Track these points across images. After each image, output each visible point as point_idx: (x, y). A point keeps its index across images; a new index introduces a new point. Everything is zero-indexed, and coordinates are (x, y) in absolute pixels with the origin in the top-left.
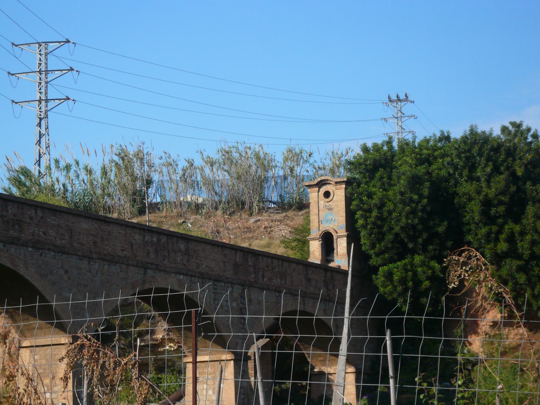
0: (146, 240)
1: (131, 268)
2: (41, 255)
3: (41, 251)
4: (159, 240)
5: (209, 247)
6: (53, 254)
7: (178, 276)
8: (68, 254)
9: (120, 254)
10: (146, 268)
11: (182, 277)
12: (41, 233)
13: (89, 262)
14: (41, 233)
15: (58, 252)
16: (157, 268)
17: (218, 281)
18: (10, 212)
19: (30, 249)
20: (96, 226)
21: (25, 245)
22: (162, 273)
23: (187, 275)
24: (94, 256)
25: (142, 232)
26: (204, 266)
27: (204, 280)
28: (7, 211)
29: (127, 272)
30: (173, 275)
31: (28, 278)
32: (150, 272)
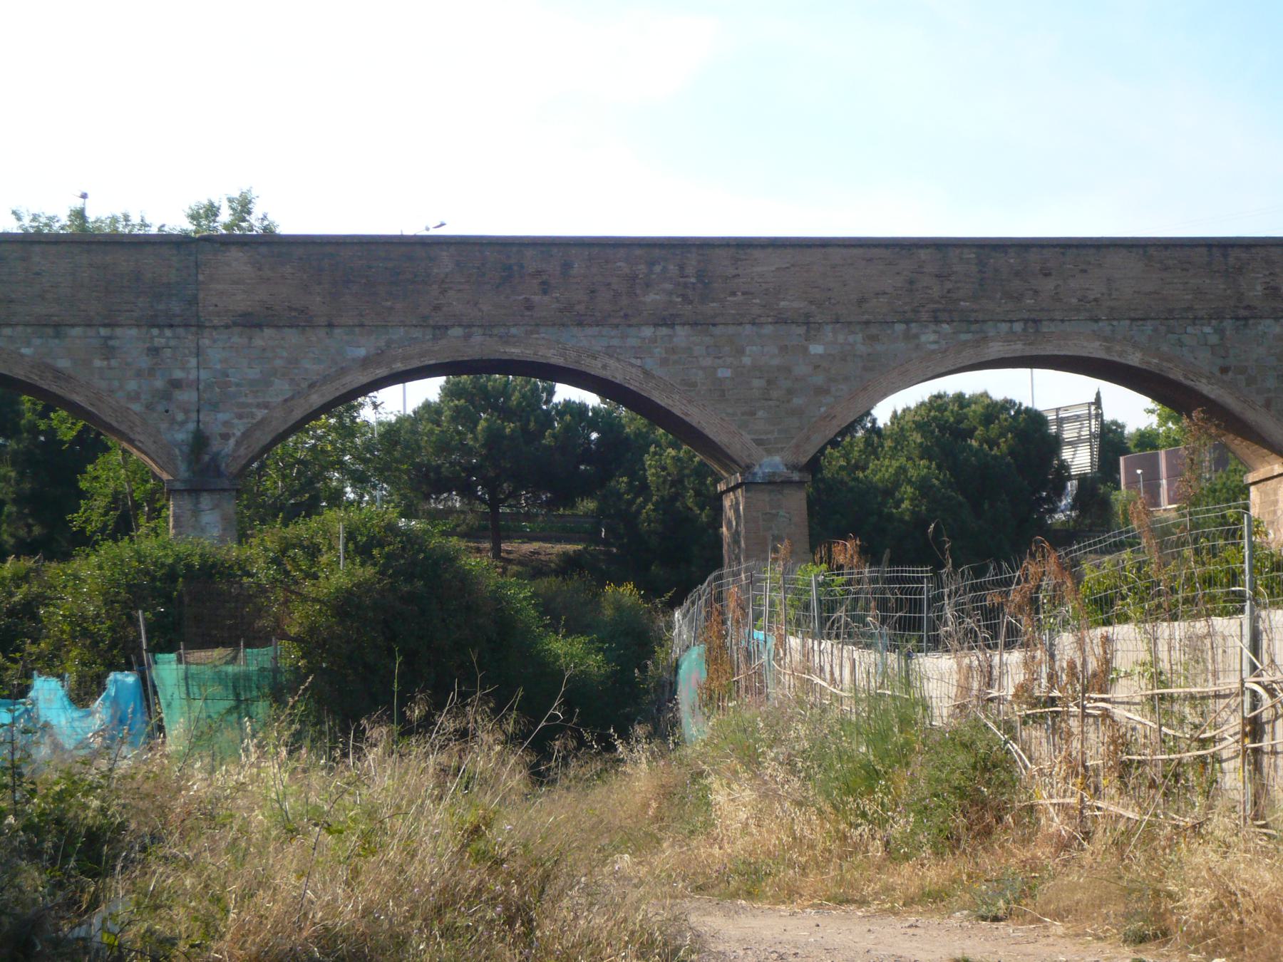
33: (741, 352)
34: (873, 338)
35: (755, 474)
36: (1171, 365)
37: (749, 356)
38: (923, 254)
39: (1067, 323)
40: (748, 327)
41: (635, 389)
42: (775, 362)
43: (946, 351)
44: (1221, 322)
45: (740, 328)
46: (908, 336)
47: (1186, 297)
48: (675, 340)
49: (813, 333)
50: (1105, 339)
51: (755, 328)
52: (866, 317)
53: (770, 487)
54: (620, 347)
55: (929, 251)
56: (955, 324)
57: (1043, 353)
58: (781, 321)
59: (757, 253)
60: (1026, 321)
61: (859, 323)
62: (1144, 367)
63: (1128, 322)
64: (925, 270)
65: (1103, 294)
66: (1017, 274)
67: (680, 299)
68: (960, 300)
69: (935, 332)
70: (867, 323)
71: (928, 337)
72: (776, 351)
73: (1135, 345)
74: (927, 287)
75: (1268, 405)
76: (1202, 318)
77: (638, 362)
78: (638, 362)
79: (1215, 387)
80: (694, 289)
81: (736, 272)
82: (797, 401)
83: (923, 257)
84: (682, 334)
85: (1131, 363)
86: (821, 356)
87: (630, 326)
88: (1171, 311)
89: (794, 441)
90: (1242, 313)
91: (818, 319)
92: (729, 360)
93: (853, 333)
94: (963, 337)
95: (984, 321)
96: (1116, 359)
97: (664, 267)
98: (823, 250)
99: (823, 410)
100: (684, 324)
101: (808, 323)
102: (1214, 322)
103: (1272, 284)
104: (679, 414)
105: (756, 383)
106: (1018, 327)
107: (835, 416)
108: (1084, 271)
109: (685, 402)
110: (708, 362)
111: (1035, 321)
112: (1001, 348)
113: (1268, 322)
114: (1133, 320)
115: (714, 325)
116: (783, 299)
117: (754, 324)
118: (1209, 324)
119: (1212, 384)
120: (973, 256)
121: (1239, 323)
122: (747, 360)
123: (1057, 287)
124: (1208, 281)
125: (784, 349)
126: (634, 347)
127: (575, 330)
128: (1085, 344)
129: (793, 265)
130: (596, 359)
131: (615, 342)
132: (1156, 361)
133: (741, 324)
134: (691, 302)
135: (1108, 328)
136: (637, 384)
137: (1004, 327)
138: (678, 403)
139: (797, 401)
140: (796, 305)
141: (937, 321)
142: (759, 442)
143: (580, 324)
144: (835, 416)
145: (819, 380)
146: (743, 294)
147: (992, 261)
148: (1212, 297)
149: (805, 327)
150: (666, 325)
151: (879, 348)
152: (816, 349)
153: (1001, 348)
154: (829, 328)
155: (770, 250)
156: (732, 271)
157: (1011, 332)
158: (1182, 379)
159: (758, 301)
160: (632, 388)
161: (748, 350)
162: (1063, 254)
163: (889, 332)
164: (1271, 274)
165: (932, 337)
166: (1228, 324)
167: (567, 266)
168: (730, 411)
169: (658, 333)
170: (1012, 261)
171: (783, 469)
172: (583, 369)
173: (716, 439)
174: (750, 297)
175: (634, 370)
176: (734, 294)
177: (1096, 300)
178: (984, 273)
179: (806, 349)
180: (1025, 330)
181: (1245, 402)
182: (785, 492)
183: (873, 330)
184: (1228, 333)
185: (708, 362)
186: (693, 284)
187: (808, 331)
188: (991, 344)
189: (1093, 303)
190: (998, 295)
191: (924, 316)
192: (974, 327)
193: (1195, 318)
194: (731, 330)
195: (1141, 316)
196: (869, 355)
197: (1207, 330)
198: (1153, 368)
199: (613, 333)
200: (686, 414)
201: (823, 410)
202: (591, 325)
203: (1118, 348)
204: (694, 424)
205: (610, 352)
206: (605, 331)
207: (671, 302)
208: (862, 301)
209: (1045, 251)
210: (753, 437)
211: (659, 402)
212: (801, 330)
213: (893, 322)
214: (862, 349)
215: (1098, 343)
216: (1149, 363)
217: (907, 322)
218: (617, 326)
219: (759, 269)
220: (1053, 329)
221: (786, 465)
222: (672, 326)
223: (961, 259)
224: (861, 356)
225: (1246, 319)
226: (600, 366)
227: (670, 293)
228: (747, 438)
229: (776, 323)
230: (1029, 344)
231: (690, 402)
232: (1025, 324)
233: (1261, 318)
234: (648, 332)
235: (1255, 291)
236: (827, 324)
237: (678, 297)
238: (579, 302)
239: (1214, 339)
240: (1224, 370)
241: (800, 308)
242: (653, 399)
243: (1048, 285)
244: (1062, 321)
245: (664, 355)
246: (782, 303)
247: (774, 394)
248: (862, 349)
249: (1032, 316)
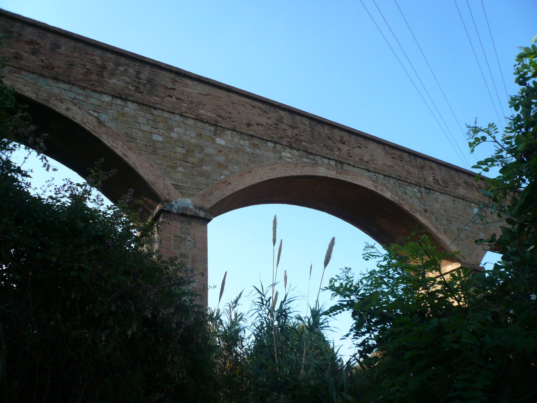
33: (170, 129)
34: (256, 146)
35: (172, 206)
36: (404, 203)
37: (177, 133)
39: (356, 168)
40: (178, 117)
41: (89, 129)
42: (193, 141)
43: (296, 164)
44: (421, 188)
45: (172, 116)
46: (274, 150)
47: (404, 173)
48: (126, 109)
49: (219, 132)
50: (374, 181)
51: (182, 119)
52: (251, 133)
53: (182, 218)
54: (83, 101)
55: (285, 113)
56: (300, 152)
57: (346, 180)
58: (199, 119)
59: (188, 82)
61: (247, 135)
62: (392, 200)
63: (382, 176)
64: (283, 121)
65: (369, 160)
66: (330, 139)
67: (133, 88)
68: (303, 141)
69: (289, 152)
70: (252, 136)
71: (286, 154)
72: (195, 136)
73: (387, 188)
74: (285, 129)
75: (445, 232)
76: (413, 184)
77: (96, 114)
78: (96, 114)
79: (423, 218)
80: (144, 86)
81: (173, 87)
82: (206, 168)
83: (282, 115)
84: (131, 108)
85: (387, 197)
86: (223, 146)
87: (94, 91)
88: (400, 176)
89: (202, 192)
91: (223, 125)
92: (162, 132)
93: (243, 139)
94: (305, 160)
95: (316, 155)
96: (380, 193)
97: (126, 69)
98: (228, 93)
99: (222, 177)
100: (134, 102)
101: (216, 126)
102: (418, 187)
103: (435, 178)
104: (120, 154)
105: (179, 150)
107: (230, 183)
109: (125, 147)
110: (147, 128)
111: (340, 162)
112: (325, 171)
113: (438, 193)
114: (385, 175)
115: (155, 109)
116: (202, 109)
117: (181, 116)
118: (416, 188)
119: (422, 216)
120: (308, 123)
121: (427, 191)
122: (174, 135)
123: (349, 150)
124: (411, 169)
125: (200, 135)
126: (94, 105)
127: (50, 82)
128: (365, 181)
129: (209, 95)
130: (62, 103)
131: (81, 98)
132: (397, 198)
133: (173, 113)
134: (141, 92)
135: (375, 177)
136: (91, 127)
137: (326, 161)
138: (120, 147)
139: (206, 168)
140: (209, 114)
142: (177, 187)
143: (56, 79)
144: (230, 183)
145: (221, 159)
146: (177, 98)
147: (317, 128)
148: (414, 176)
149: (214, 128)
150: (121, 98)
151: (258, 152)
152: (220, 141)
153: (325, 171)
154: (229, 132)
155: (196, 83)
156: (170, 85)
157: (329, 164)
158: (409, 210)
159: (185, 105)
160: (86, 128)
161: (176, 129)
162: (350, 136)
163: (264, 145)
164: (434, 174)
165: (289, 155)
167: (55, 46)
168: (158, 161)
169: (113, 102)
170: (327, 131)
171: (191, 207)
172: (50, 105)
173: (146, 177)
174: (180, 101)
175: (91, 118)
176: (171, 97)
177: (367, 161)
178: (314, 132)
179: (214, 140)
180: (336, 165)
181: (436, 228)
182: (193, 224)
183: (256, 141)
184: (424, 194)
185: (147, 128)
186: (144, 83)
187: (216, 129)
188: (320, 168)
189: (366, 163)
190: (322, 145)
192: (310, 156)
194: (166, 115)
195: (388, 175)
196: (252, 154)
198: (396, 202)
199: (81, 92)
200: (125, 156)
201: (222, 177)
202: (64, 82)
203: (380, 187)
204: (131, 163)
205: (75, 102)
206: (75, 89)
207: (127, 88)
208: (249, 125)
209: (342, 132)
210: (173, 182)
211: (106, 142)
212: (212, 129)
213: (267, 141)
214: (249, 150)
215: (371, 182)
216: (394, 199)
217: (275, 143)
218: (84, 88)
219: (188, 90)
220: (349, 169)
221: (195, 206)
222: (126, 100)
223: (302, 122)
224: (248, 153)
225: (429, 189)
226: (64, 107)
227: (128, 83)
228: (168, 182)
229: (197, 119)
230: (339, 173)
231: (129, 149)
232: (336, 163)
233: (435, 191)
234: (107, 99)
236: (228, 129)
237: (132, 86)
238: (59, 67)
239: (419, 195)
241: (211, 117)
242: (102, 139)
243: (345, 148)
244: (354, 166)
245: (116, 115)
246: (201, 111)
247: (191, 159)
248: (249, 150)
249: (339, 159)
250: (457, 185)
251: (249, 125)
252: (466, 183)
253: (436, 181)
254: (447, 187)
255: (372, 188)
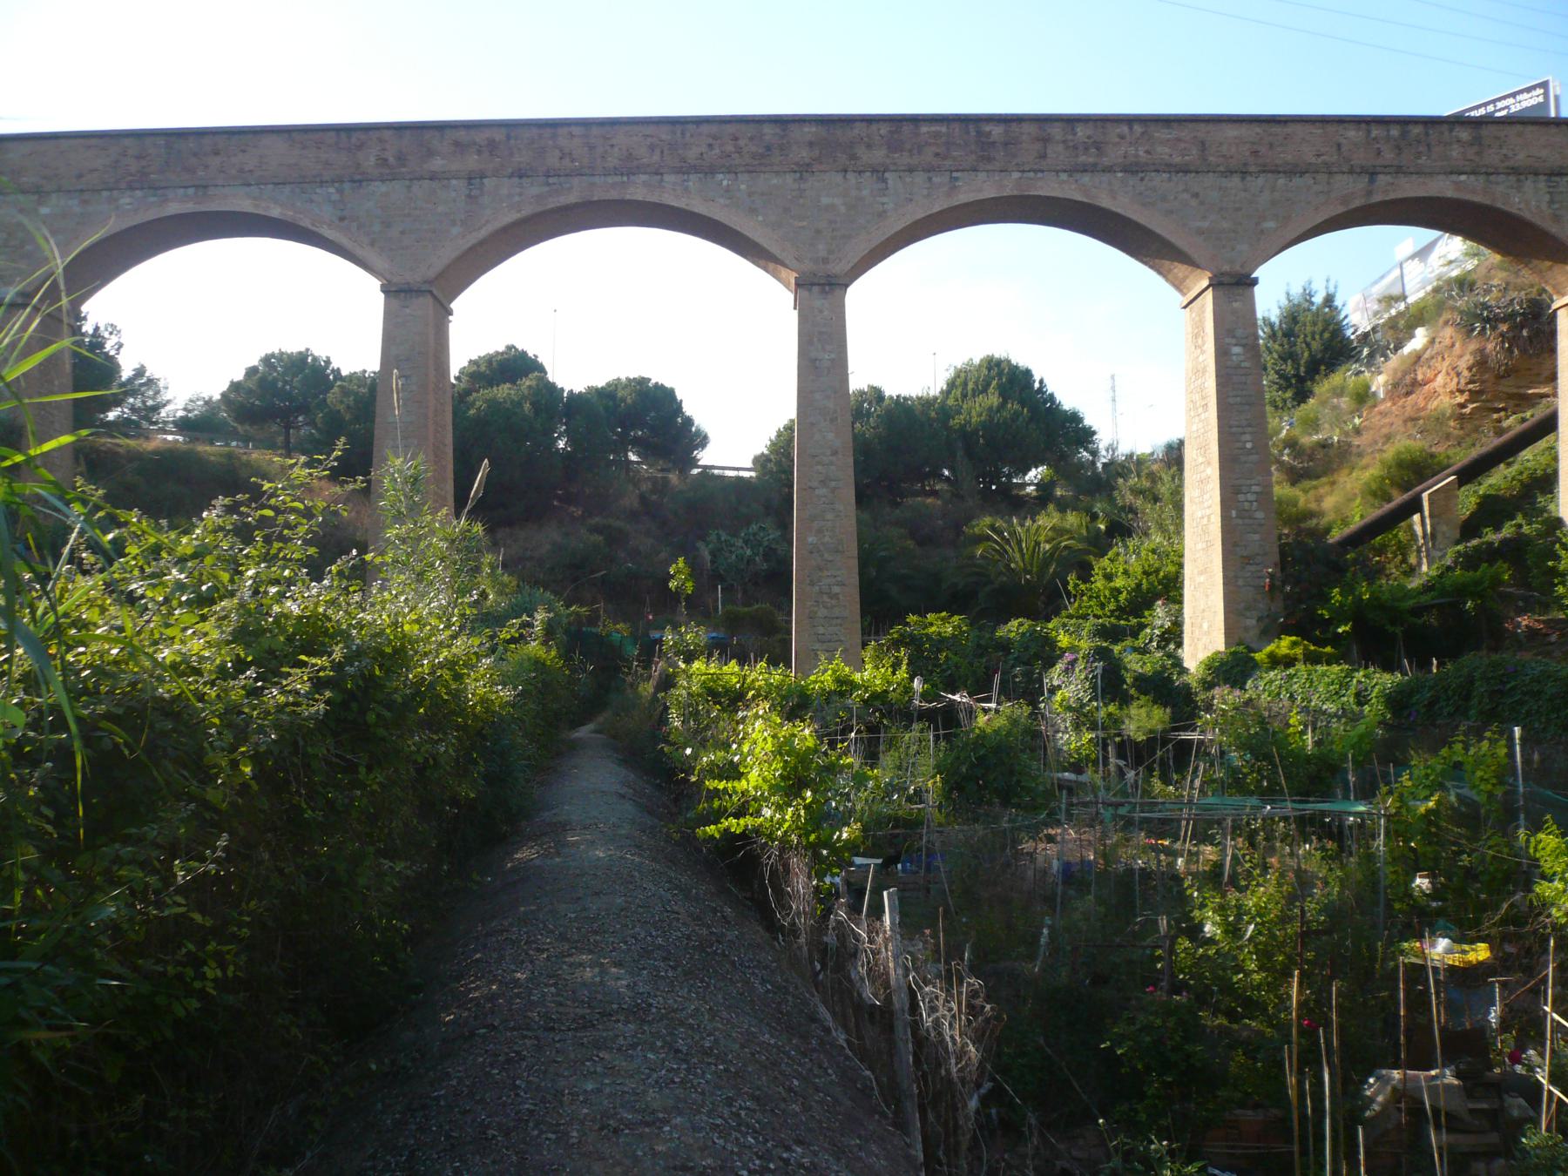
0: (1373, 135)
1: (1338, 177)
2: (1142, 179)
3: (1141, 175)
4: (1404, 134)
5: (1530, 128)
6: (1165, 176)
7: (1454, 177)
8: (1197, 172)
9: (1313, 160)
10: (1373, 174)
11: (1463, 178)
12: (1141, 153)
13: (1243, 179)
14: (1141, 153)
15: (1178, 172)
16: (1399, 170)
17: (1560, 174)
18: (1080, 134)
19: (1120, 175)
20: (1258, 130)
21: (1109, 170)
22: (1414, 176)
23: (1473, 173)
24: (1252, 169)
25: (1363, 125)
26: (1521, 156)
27: (1522, 177)
28: (1075, 134)
29: (1328, 183)
30: (1441, 177)
31: (1119, 211)
32: (1382, 180)
34: (85, 202)
38: (127, 142)
50: (255, 199)
60: (196, 187)
63: (271, 186)
66: (195, 155)
71: (125, 200)
75: (372, 244)
90: (358, 177)
94: (152, 199)
102: (336, 185)
106: (191, 191)
108: (244, 151)
113: (377, 183)
141: (132, 188)
152: (44, 210)
154: (54, 195)
165: (128, 200)
166: (347, 186)
177: (251, 171)
191: (123, 185)
192: (160, 192)
193: (322, 182)
197: (332, 190)
208: (80, 176)
225: (360, 181)
235: (369, 161)
239: (336, 197)
240: (342, 219)
243: (215, 162)
250: (431, 153)
251: (80, 176)
252: (457, 144)
253: (383, 162)
254: (404, 166)
255: (250, 209)
